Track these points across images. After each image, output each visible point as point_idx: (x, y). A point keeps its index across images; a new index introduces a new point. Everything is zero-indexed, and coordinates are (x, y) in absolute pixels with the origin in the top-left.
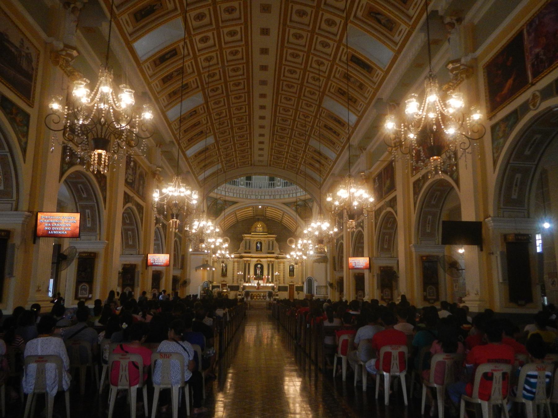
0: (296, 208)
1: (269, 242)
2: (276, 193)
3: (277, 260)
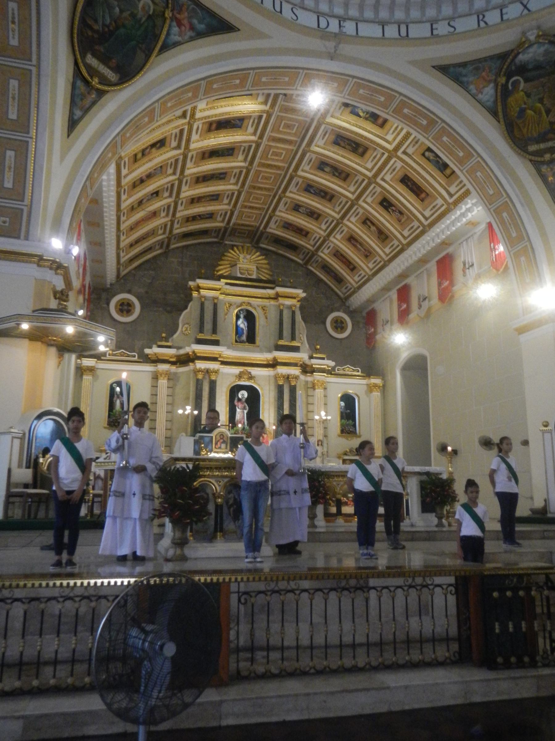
0: (505, 86)
1: (281, 312)
2: (415, 14)
3: (302, 377)
